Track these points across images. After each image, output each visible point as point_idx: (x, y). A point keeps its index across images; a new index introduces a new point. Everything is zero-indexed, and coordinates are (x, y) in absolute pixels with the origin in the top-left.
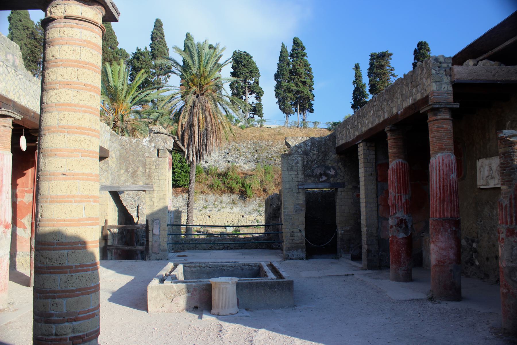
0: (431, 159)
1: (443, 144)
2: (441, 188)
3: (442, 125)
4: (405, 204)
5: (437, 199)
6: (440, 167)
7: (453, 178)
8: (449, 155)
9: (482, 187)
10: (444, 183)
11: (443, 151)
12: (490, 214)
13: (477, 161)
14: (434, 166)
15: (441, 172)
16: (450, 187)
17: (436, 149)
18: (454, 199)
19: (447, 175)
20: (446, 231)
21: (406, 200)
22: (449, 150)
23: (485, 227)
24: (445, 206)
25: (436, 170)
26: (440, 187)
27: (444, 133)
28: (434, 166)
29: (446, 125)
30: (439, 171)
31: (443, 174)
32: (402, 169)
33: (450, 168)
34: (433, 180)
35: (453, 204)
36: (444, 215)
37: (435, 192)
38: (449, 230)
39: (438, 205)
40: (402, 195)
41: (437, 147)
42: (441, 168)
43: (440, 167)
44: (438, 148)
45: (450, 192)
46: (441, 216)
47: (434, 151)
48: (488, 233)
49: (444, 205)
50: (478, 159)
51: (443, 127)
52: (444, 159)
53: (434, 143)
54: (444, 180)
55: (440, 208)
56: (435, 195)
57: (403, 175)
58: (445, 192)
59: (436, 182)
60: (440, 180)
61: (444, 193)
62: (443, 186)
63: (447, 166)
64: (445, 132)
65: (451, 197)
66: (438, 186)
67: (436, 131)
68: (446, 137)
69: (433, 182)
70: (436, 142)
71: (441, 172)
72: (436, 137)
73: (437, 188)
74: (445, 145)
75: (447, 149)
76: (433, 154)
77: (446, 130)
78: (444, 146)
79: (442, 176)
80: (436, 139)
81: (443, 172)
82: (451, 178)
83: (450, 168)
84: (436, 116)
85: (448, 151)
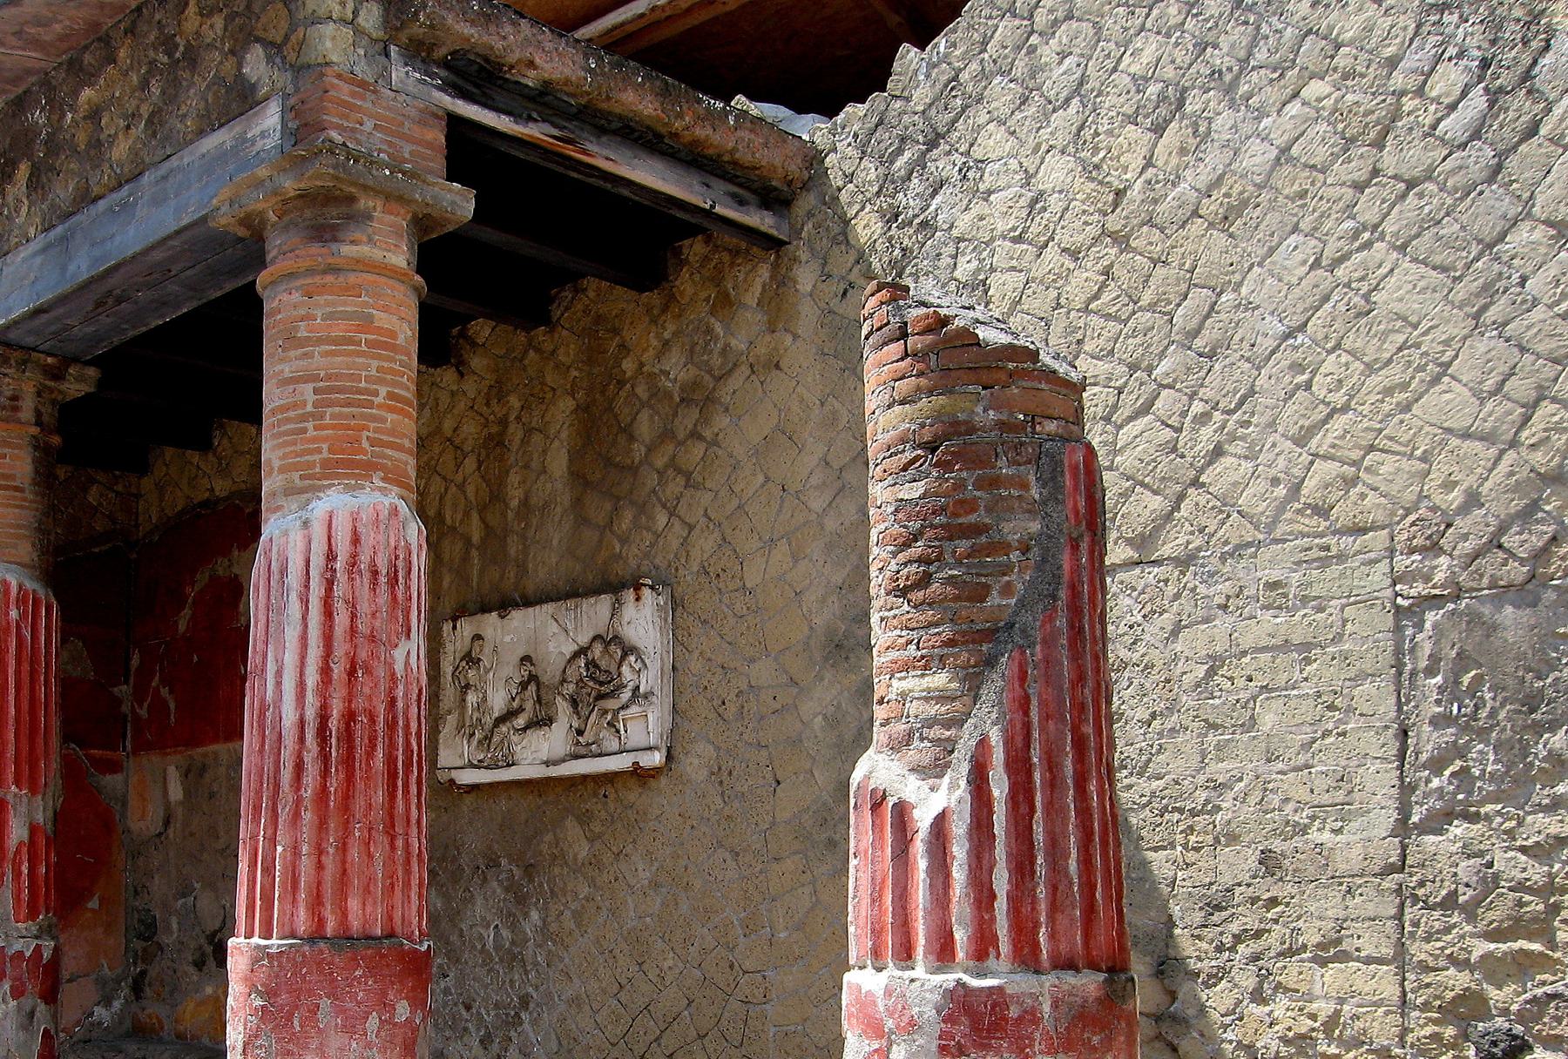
0: (271, 528)
1: (365, 433)
2: (333, 724)
3: (366, 304)
4: (25, 857)
5: (298, 802)
6: (330, 584)
7: (407, 663)
8: (394, 511)
9: (468, 777)
10: (350, 698)
11: (357, 477)
12: (505, 933)
13: (447, 627)
14: (294, 579)
15: (341, 620)
16: (391, 726)
17: (317, 457)
18: (408, 810)
19: (372, 638)
20: (351, 1027)
21: (33, 830)
22: (394, 477)
23: (468, 1008)
24: (354, 853)
25: (305, 602)
26: (323, 718)
27: (375, 363)
28: (294, 579)
29: (385, 309)
30: (328, 613)
31: (353, 630)
32: (18, 627)
33: (394, 598)
34: (279, 674)
35: (400, 843)
36: (344, 914)
37: (287, 755)
38: (373, 1022)
39: (305, 849)
40: (10, 798)
41: (319, 451)
42: (338, 591)
43: (330, 584)
44: (325, 455)
45: (391, 761)
46: (321, 922)
47: (296, 476)
48: (485, 1042)
49: (343, 848)
50: (455, 619)
51: (366, 324)
52: (361, 529)
53: (304, 418)
54: (352, 673)
55: (320, 866)
56: (286, 775)
57: (26, 667)
58: (359, 752)
59: (301, 686)
60: (325, 671)
61: (348, 761)
62: (350, 717)
63: (383, 580)
64: (379, 357)
65: (392, 796)
66: (311, 713)
67: (320, 341)
68: (383, 391)
69: (279, 684)
70: (312, 415)
71: (341, 620)
72: (316, 378)
73: (302, 723)
74: (373, 442)
75: (383, 468)
76: (290, 491)
77: (384, 345)
78: (365, 444)
79: (340, 649)
80: (316, 391)
81: (353, 616)
82: (399, 668)
83: (394, 598)
84: (335, 239)
85: (384, 479)
